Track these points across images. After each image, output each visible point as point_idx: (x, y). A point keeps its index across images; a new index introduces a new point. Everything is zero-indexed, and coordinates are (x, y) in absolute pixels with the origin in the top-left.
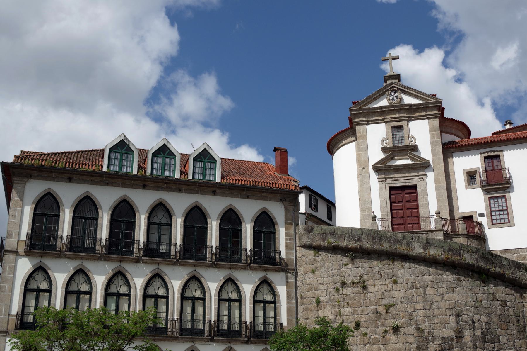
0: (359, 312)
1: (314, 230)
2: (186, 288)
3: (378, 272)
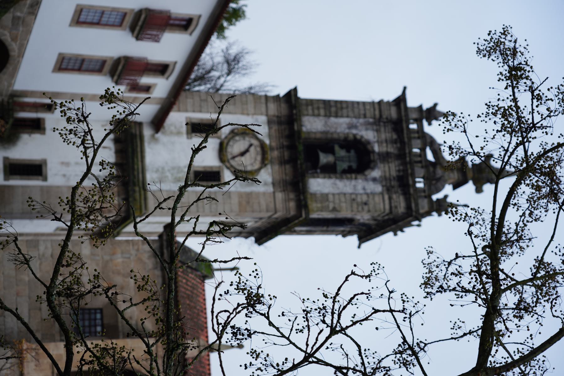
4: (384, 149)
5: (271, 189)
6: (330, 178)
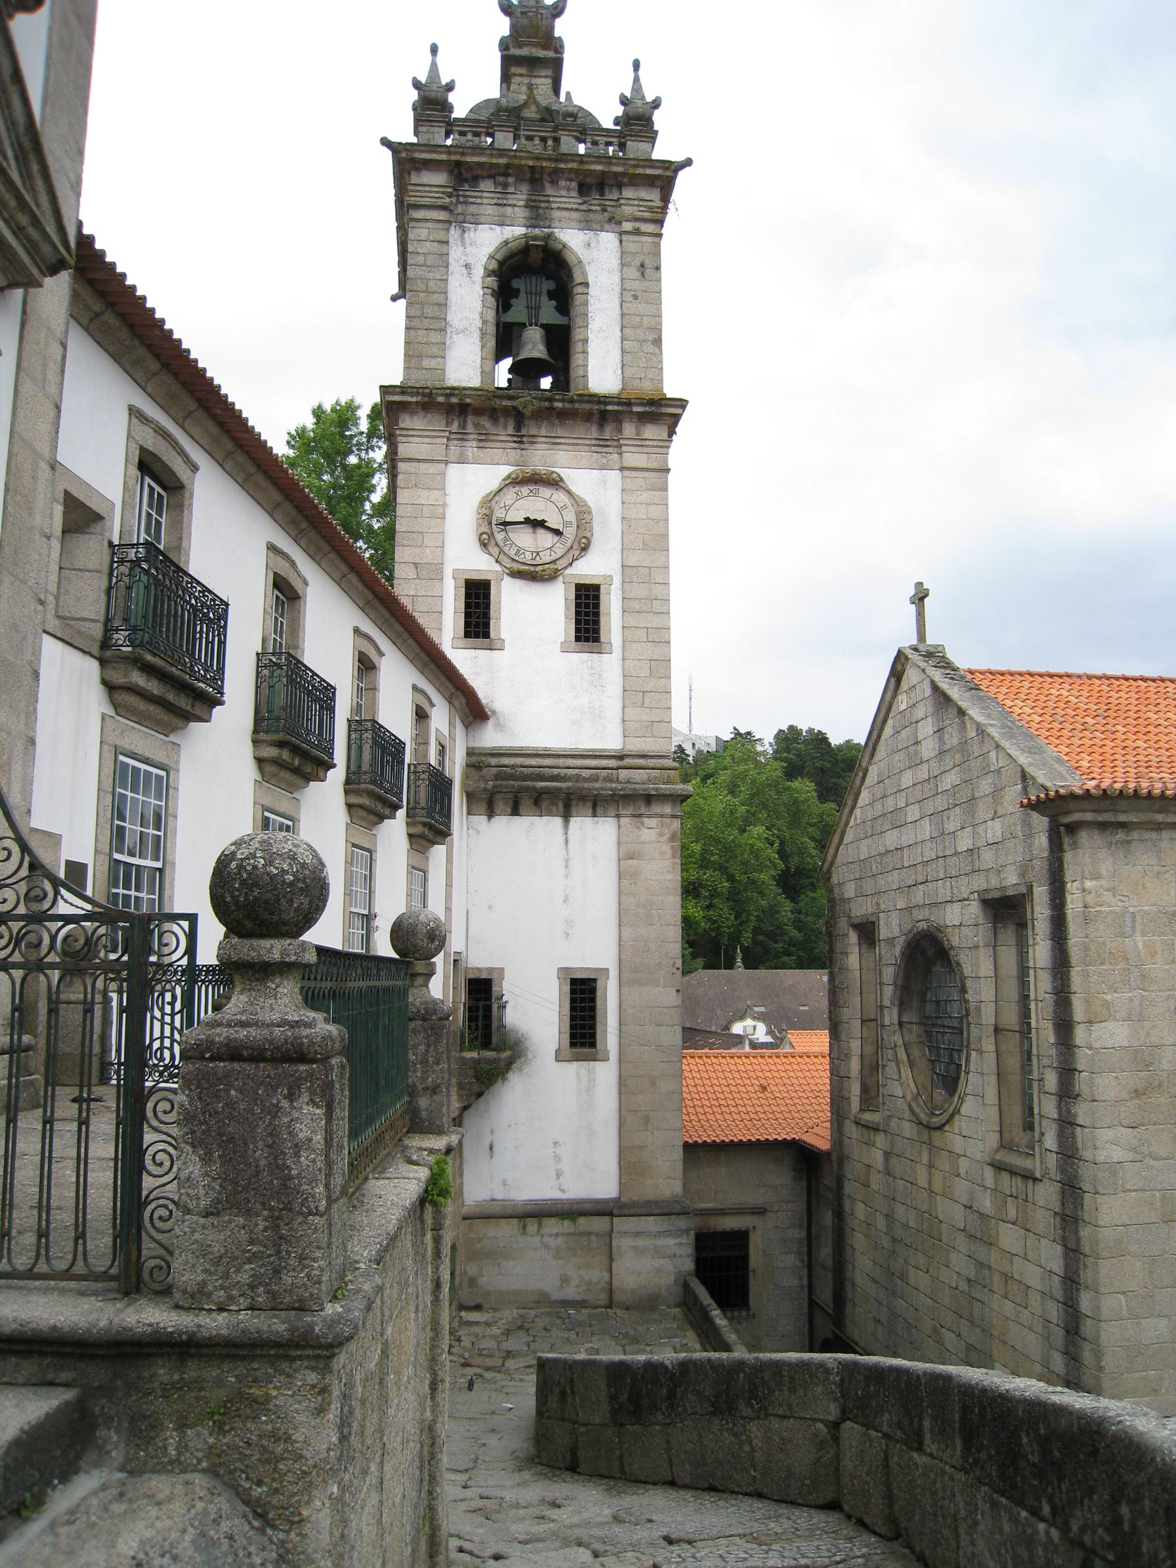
4: (521, 213)
6: (585, 341)
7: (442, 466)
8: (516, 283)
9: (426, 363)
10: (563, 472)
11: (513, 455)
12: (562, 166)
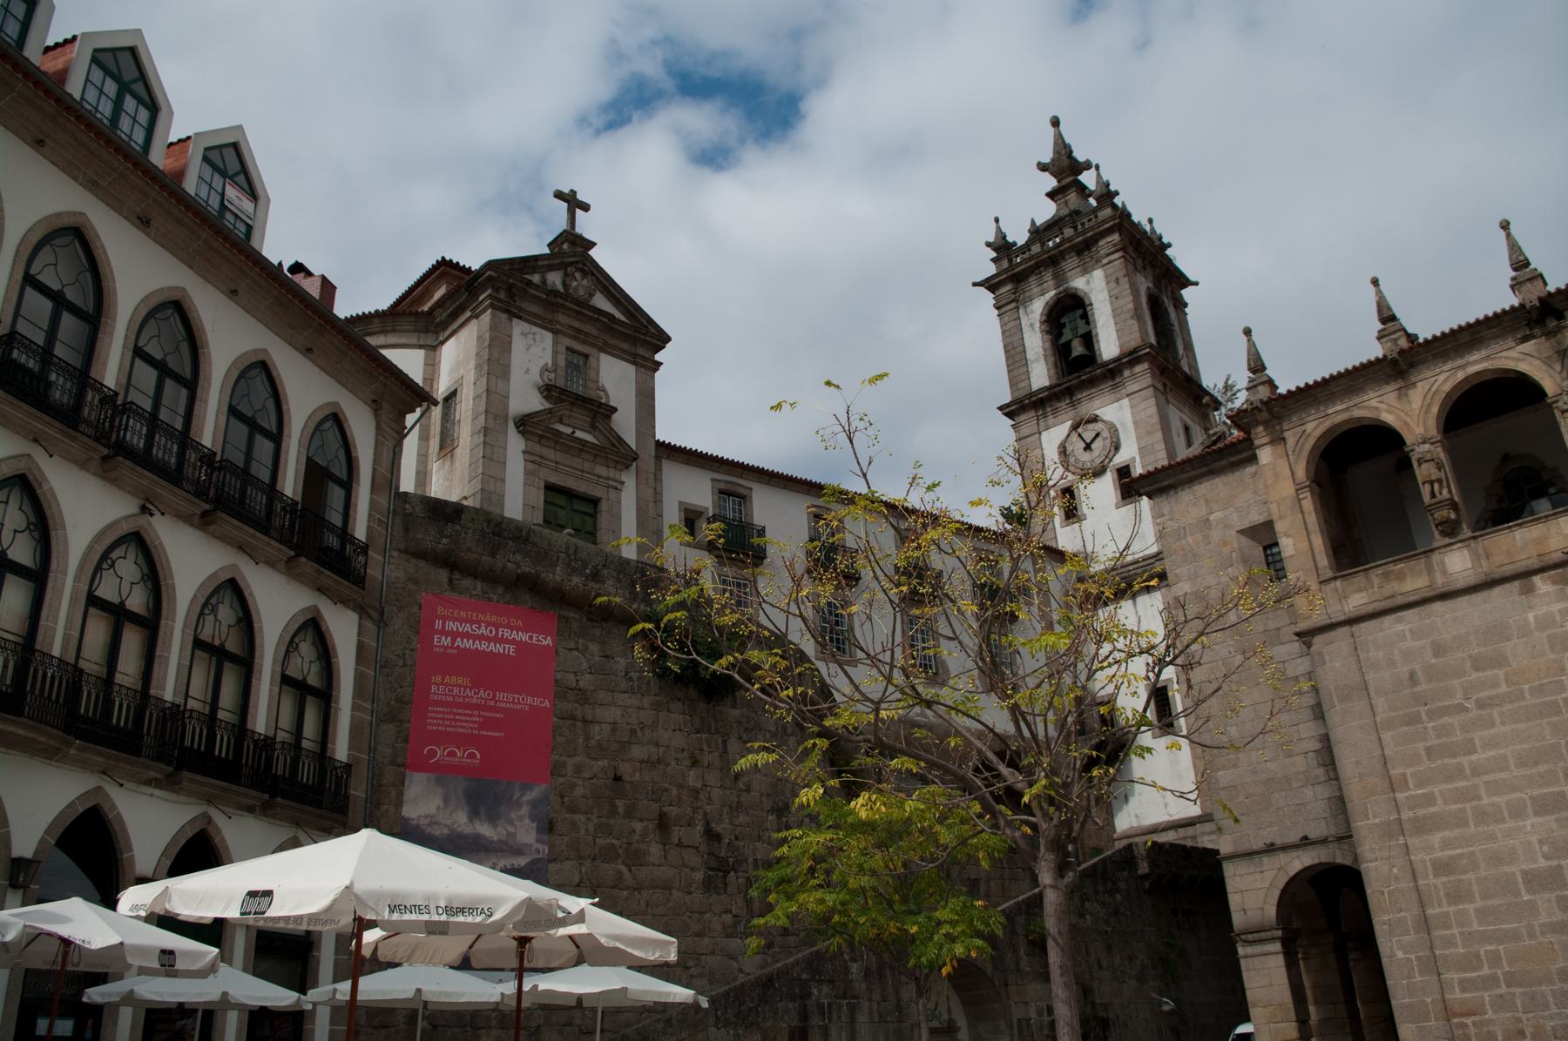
0: (570, 770)
1: (463, 516)
2: (105, 566)
3: (623, 674)
4: (1051, 283)
5: (1125, 402)
6: (1097, 335)
7: (1037, 435)
8: (1062, 321)
9: (1020, 386)
10: (1097, 412)
11: (1072, 414)
12: (1062, 248)
